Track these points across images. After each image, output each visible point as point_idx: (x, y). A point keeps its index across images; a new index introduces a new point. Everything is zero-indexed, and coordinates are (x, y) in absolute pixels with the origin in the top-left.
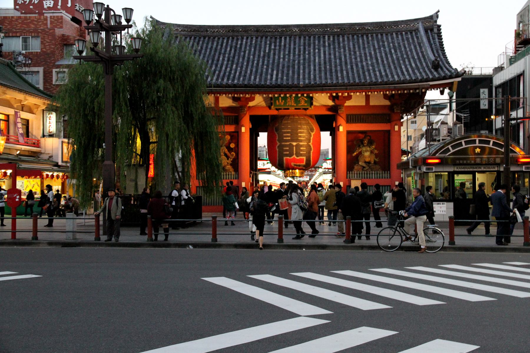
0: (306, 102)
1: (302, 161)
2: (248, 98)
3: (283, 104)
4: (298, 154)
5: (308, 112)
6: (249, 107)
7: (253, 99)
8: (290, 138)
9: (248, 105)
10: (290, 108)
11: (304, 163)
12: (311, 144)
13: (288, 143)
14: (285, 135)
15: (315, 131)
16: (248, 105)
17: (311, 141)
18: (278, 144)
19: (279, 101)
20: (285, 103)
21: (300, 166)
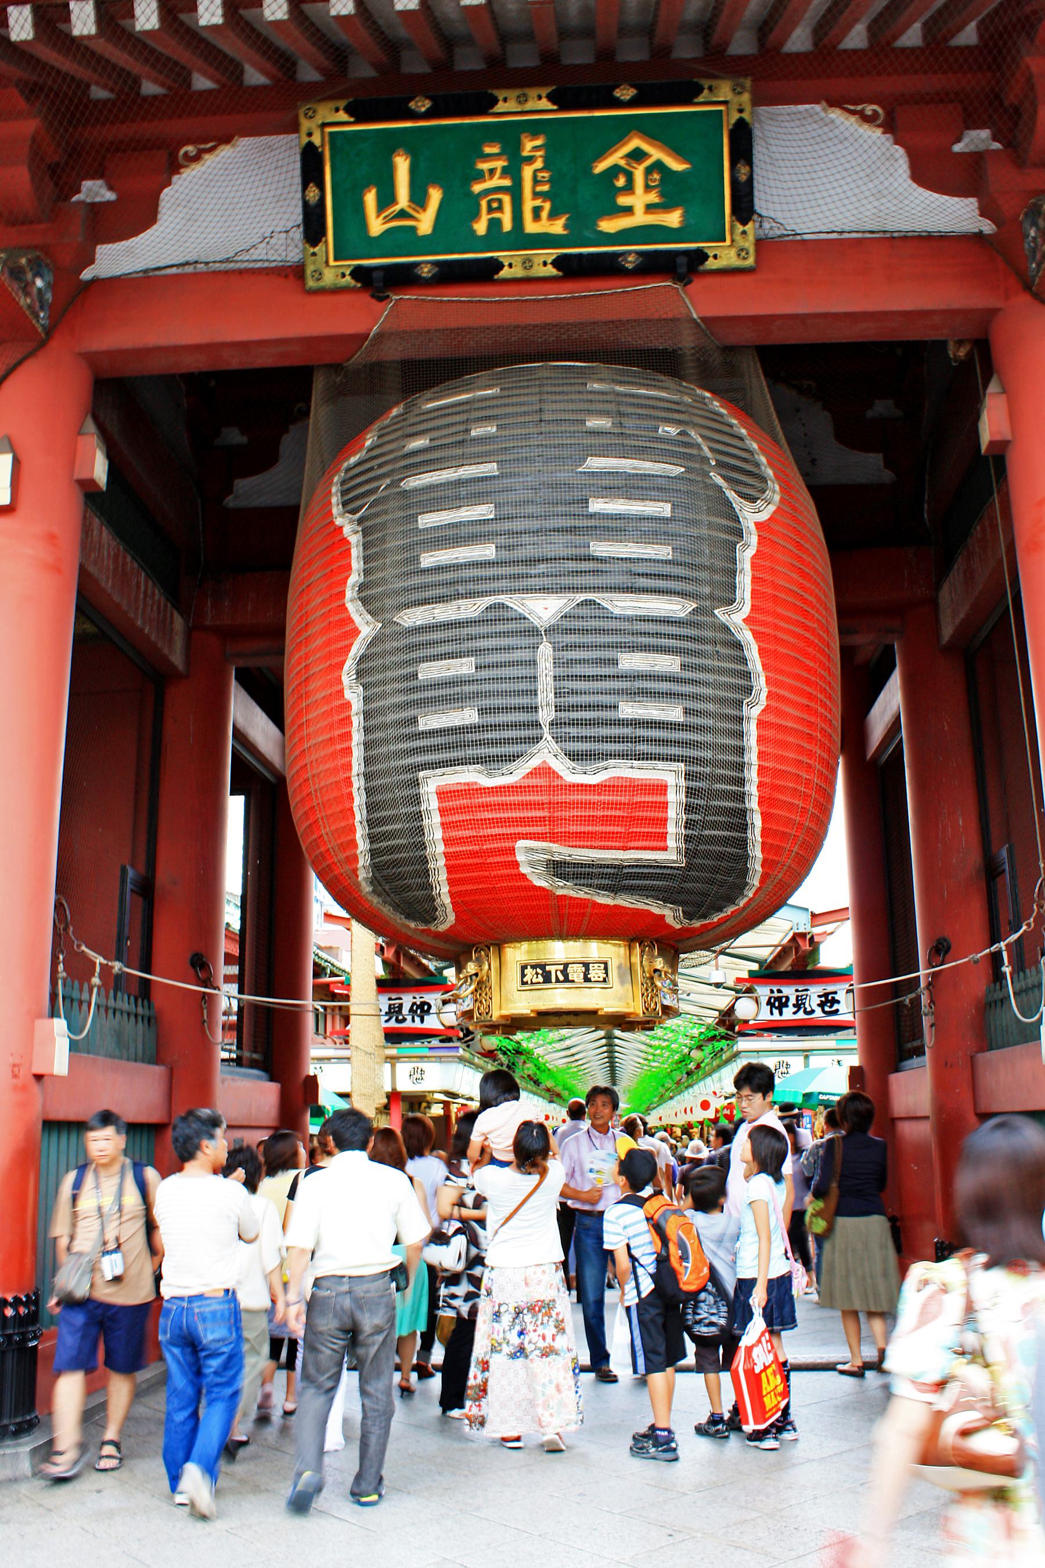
0: (671, 190)
1: (639, 813)
2: (95, 209)
3: (425, 223)
4: (589, 731)
5: (696, 303)
6: (95, 281)
7: (137, 214)
8: (487, 551)
9: (87, 275)
10: (513, 264)
11: (671, 853)
12: (736, 617)
13: (469, 609)
14: (427, 520)
15: (774, 493)
16: (87, 275)
17: (745, 582)
18: (366, 627)
19: (387, 198)
20: (459, 209)
21: (617, 879)
